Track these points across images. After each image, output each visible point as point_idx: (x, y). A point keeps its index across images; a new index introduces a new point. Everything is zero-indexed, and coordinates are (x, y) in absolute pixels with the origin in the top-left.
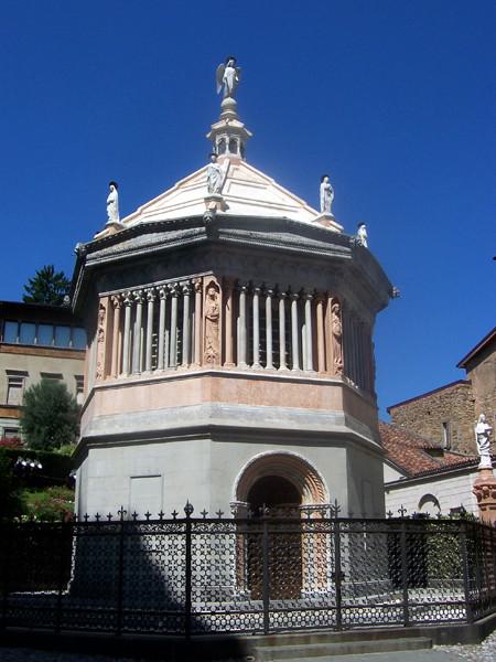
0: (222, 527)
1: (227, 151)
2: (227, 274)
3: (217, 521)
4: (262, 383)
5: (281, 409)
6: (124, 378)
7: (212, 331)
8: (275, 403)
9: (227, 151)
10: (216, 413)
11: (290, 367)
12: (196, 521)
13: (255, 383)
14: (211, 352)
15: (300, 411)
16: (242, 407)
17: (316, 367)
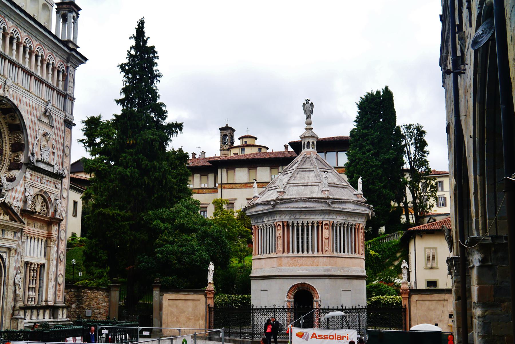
0: (262, 310)
1: (306, 148)
2: (284, 220)
3: (261, 309)
4: (296, 259)
5: (303, 267)
6: (259, 256)
7: (279, 242)
8: (301, 265)
9: (306, 148)
10: (280, 270)
11: (308, 251)
12: (255, 309)
13: (294, 259)
14: (279, 250)
15: (310, 268)
16: (289, 268)
17: (318, 251)
